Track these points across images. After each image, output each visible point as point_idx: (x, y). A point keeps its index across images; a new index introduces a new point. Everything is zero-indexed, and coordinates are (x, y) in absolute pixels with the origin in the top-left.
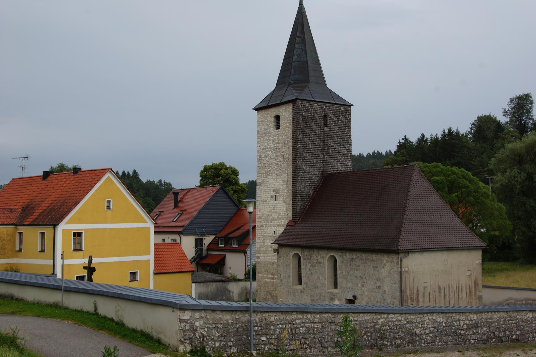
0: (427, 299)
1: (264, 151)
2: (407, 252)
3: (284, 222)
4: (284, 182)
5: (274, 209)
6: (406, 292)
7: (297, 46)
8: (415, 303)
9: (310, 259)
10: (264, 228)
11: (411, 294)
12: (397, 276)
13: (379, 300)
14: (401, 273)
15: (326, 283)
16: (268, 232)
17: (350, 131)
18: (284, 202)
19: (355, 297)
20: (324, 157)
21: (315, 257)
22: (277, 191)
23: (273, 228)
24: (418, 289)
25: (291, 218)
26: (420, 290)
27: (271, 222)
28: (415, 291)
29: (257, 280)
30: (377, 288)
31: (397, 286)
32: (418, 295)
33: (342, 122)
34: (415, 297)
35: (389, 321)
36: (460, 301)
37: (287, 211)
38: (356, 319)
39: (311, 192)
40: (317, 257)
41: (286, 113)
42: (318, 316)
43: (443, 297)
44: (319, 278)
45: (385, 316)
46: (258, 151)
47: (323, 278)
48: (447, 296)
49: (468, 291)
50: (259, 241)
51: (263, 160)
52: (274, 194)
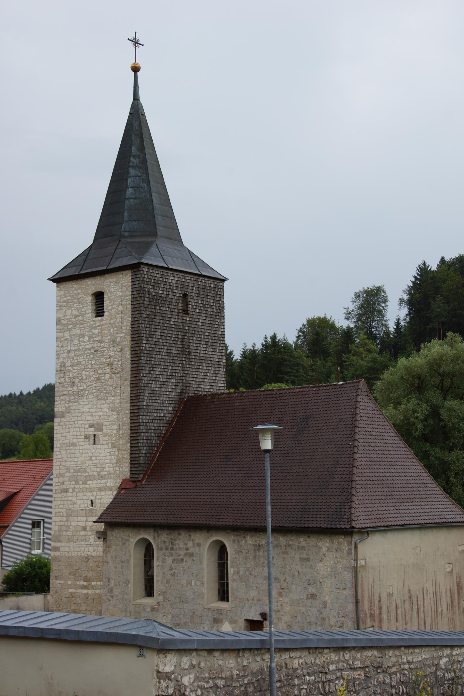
1: (72, 354)
2: (366, 532)
3: (114, 483)
4: (113, 411)
5: (91, 459)
7: (132, 171)
8: (376, 624)
9: (172, 549)
10: (69, 494)
11: (371, 608)
12: (348, 576)
13: (313, 620)
14: (355, 570)
15: (205, 591)
16: (79, 502)
17: (222, 324)
18: (113, 446)
19: (264, 615)
21: (182, 545)
22: (98, 427)
23: (90, 494)
25: (127, 475)
27: (85, 483)
28: (377, 602)
29: (52, 592)
30: (308, 598)
31: (349, 592)
32: (380, 608)
33: (211, 307)
35: (454, 662)
36: (439, 617)
37: (118, 461)
38: (410, 659)
39: (163, 428)
40: (186, 544)
41: (118, 290)
42: (359, 655)
43: (415, 612)
44: (189, 583)
45: (448, 651)
46: (58, 355)
47: (198, 583)
48: (422, 610)
49: (449, 601)
50: (60, 519)
51: (70, 371)
52: (91, 431)
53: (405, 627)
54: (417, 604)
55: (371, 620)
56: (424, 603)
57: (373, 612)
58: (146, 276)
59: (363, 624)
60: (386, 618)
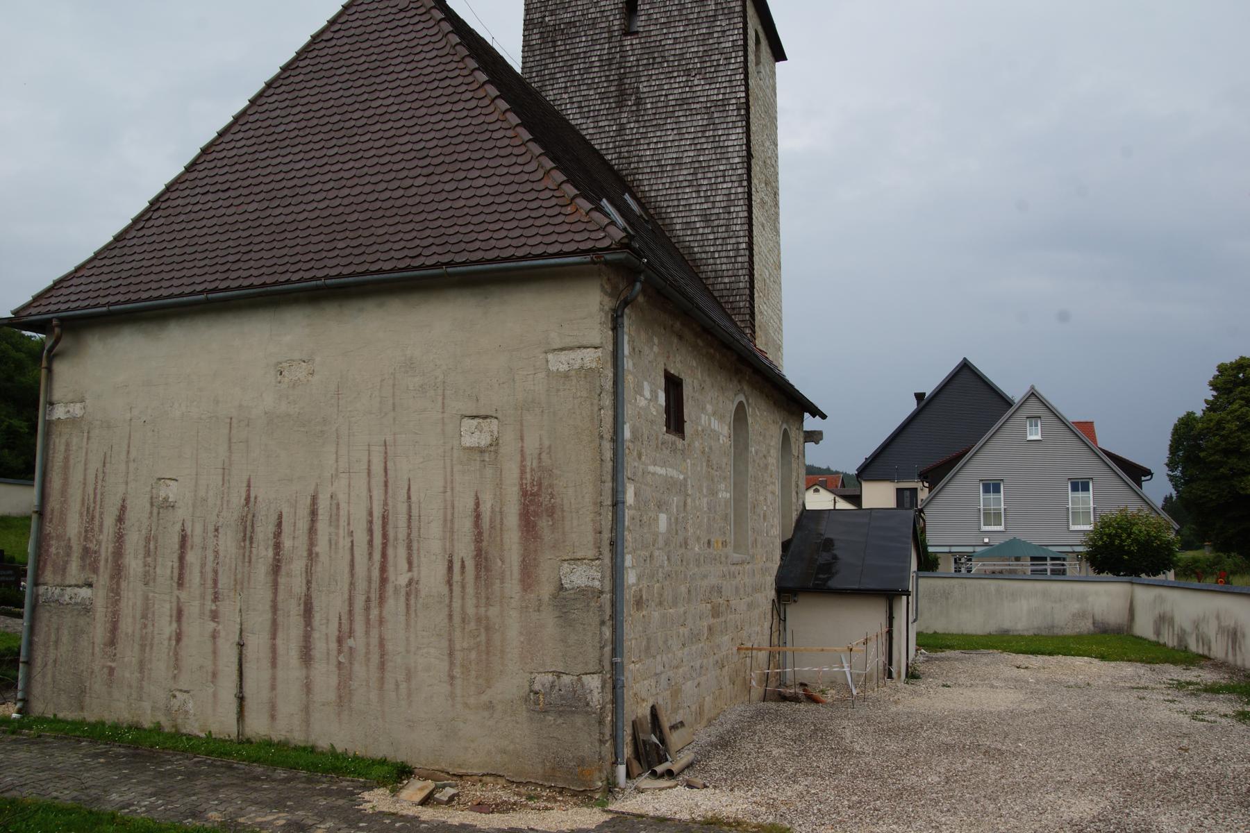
0: (166, 566)
6: (63, 521)
8: (103, 579)
20: (622, 127)
24: (123, 508)
26: (131, 516)
32: (120, 538)
34: (106, 550)
36: (394, 605)
43: (261, 571)
48: (297, 566)
49: (464, 549)
53: (209, 606)
54: (277, 546)
55: (83, 568)
56: (312, 543)
57: (92, 546)
59: (54, 572)
60: (140, 570)
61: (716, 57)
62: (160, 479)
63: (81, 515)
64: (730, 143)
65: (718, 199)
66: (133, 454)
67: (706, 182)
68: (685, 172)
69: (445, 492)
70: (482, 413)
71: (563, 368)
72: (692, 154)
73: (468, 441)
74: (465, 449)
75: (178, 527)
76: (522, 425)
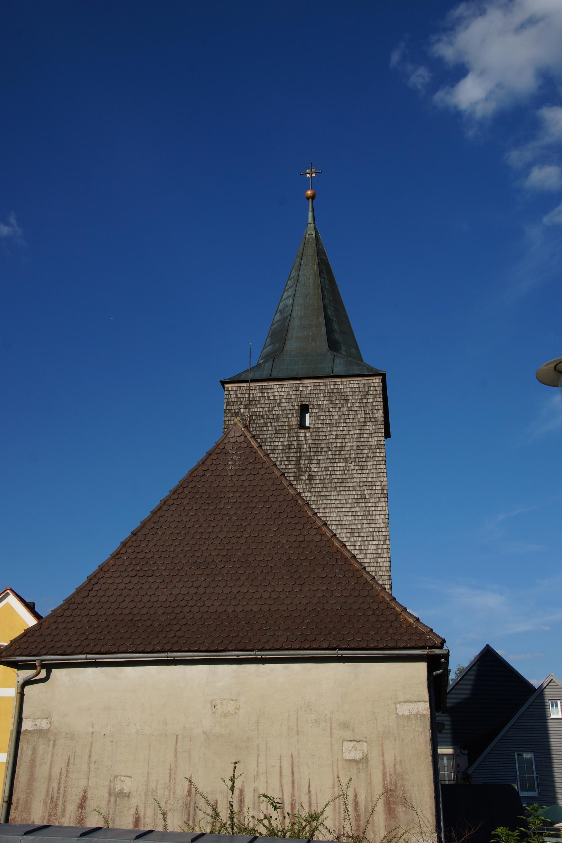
24: (84, 798)
58: (233, 396)
61: (366, 451)
62: (116, 776)
63: (45, 802)
64: (377, 513)
65: (369, 551)
66: (93, 759)
67: (360, 539)
68: (345, 531)
69: (334, 788)
70: (357, 738)
71: (407, 713)
72: (350, 518)
73: (348, 756)
74: (346, 760)
75: (133, 811)
76: (382, 746)
